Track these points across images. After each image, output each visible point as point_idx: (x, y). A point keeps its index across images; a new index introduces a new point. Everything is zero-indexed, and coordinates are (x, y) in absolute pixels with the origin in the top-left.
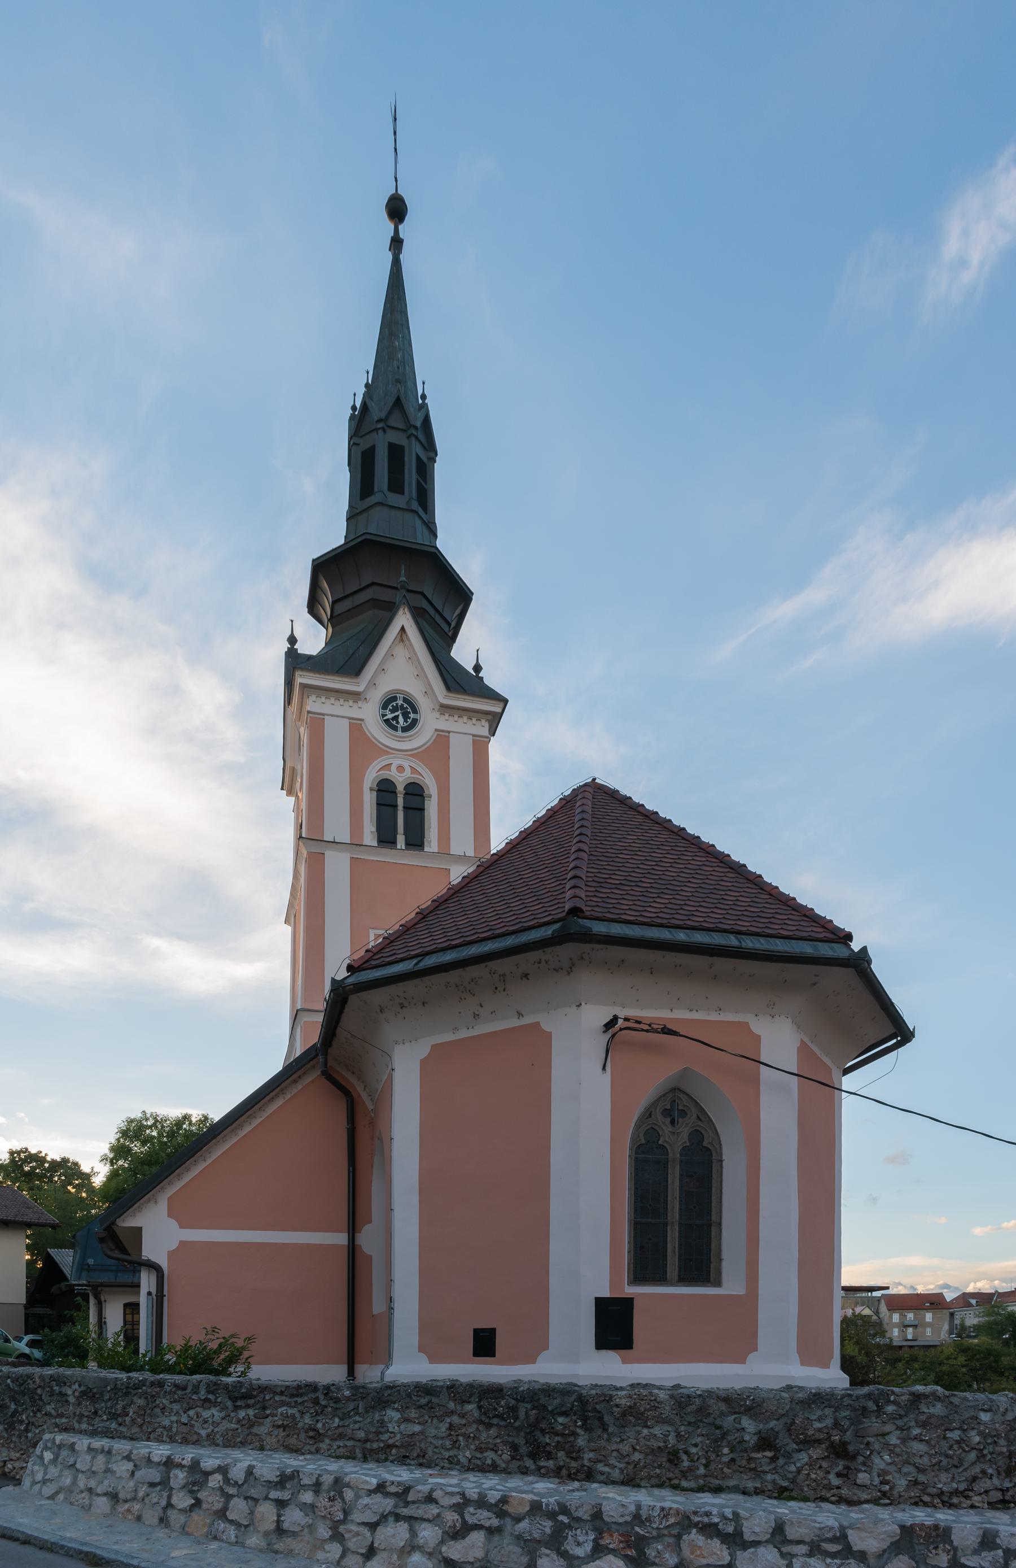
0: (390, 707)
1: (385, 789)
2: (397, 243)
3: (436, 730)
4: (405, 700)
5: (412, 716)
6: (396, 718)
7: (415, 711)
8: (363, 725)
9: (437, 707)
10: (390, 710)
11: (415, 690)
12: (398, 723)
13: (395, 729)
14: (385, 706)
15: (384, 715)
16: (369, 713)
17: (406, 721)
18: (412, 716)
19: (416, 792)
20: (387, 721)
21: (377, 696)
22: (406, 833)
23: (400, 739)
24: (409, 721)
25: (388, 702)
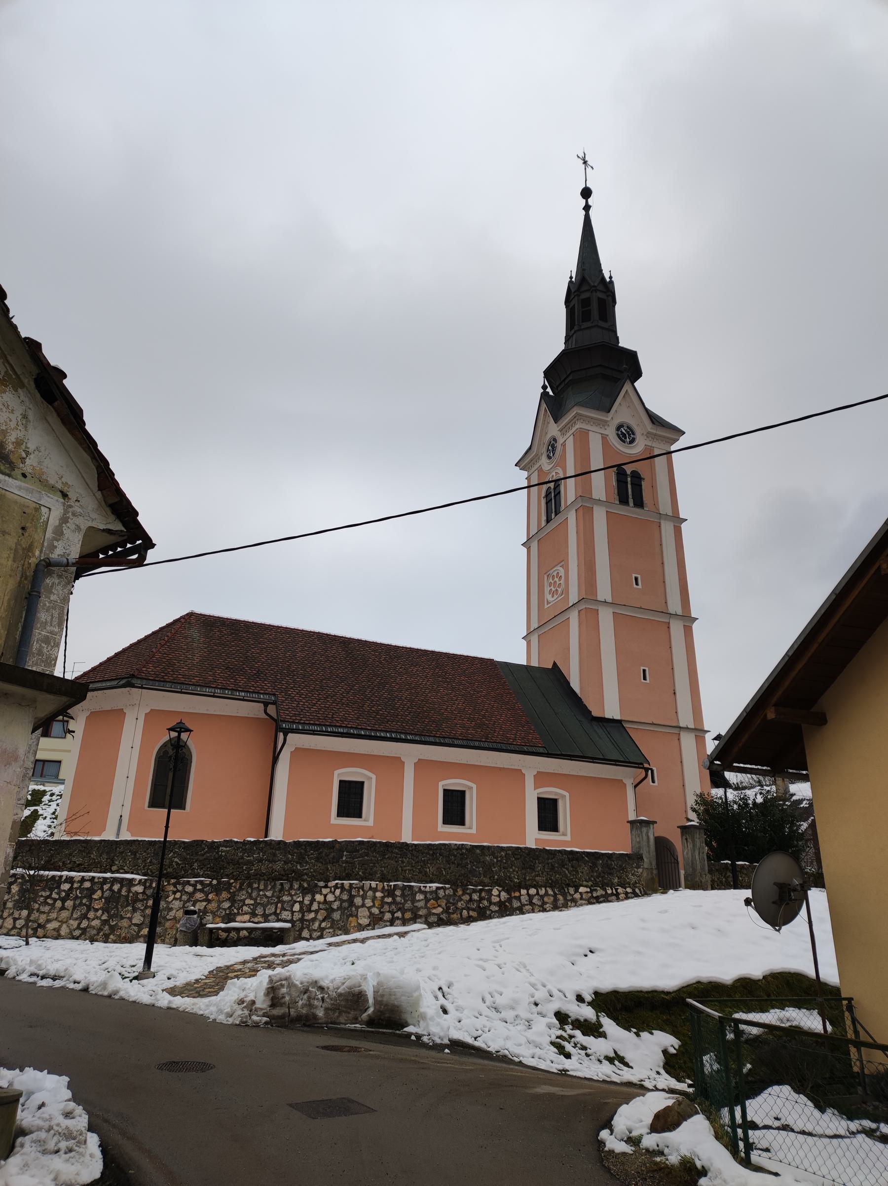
2: (587, 208)
4: (628, 427)
11: (633, 423)
16: (611, 433)
23: (631, 448)
24: (631, 438)
25: (619, 428)
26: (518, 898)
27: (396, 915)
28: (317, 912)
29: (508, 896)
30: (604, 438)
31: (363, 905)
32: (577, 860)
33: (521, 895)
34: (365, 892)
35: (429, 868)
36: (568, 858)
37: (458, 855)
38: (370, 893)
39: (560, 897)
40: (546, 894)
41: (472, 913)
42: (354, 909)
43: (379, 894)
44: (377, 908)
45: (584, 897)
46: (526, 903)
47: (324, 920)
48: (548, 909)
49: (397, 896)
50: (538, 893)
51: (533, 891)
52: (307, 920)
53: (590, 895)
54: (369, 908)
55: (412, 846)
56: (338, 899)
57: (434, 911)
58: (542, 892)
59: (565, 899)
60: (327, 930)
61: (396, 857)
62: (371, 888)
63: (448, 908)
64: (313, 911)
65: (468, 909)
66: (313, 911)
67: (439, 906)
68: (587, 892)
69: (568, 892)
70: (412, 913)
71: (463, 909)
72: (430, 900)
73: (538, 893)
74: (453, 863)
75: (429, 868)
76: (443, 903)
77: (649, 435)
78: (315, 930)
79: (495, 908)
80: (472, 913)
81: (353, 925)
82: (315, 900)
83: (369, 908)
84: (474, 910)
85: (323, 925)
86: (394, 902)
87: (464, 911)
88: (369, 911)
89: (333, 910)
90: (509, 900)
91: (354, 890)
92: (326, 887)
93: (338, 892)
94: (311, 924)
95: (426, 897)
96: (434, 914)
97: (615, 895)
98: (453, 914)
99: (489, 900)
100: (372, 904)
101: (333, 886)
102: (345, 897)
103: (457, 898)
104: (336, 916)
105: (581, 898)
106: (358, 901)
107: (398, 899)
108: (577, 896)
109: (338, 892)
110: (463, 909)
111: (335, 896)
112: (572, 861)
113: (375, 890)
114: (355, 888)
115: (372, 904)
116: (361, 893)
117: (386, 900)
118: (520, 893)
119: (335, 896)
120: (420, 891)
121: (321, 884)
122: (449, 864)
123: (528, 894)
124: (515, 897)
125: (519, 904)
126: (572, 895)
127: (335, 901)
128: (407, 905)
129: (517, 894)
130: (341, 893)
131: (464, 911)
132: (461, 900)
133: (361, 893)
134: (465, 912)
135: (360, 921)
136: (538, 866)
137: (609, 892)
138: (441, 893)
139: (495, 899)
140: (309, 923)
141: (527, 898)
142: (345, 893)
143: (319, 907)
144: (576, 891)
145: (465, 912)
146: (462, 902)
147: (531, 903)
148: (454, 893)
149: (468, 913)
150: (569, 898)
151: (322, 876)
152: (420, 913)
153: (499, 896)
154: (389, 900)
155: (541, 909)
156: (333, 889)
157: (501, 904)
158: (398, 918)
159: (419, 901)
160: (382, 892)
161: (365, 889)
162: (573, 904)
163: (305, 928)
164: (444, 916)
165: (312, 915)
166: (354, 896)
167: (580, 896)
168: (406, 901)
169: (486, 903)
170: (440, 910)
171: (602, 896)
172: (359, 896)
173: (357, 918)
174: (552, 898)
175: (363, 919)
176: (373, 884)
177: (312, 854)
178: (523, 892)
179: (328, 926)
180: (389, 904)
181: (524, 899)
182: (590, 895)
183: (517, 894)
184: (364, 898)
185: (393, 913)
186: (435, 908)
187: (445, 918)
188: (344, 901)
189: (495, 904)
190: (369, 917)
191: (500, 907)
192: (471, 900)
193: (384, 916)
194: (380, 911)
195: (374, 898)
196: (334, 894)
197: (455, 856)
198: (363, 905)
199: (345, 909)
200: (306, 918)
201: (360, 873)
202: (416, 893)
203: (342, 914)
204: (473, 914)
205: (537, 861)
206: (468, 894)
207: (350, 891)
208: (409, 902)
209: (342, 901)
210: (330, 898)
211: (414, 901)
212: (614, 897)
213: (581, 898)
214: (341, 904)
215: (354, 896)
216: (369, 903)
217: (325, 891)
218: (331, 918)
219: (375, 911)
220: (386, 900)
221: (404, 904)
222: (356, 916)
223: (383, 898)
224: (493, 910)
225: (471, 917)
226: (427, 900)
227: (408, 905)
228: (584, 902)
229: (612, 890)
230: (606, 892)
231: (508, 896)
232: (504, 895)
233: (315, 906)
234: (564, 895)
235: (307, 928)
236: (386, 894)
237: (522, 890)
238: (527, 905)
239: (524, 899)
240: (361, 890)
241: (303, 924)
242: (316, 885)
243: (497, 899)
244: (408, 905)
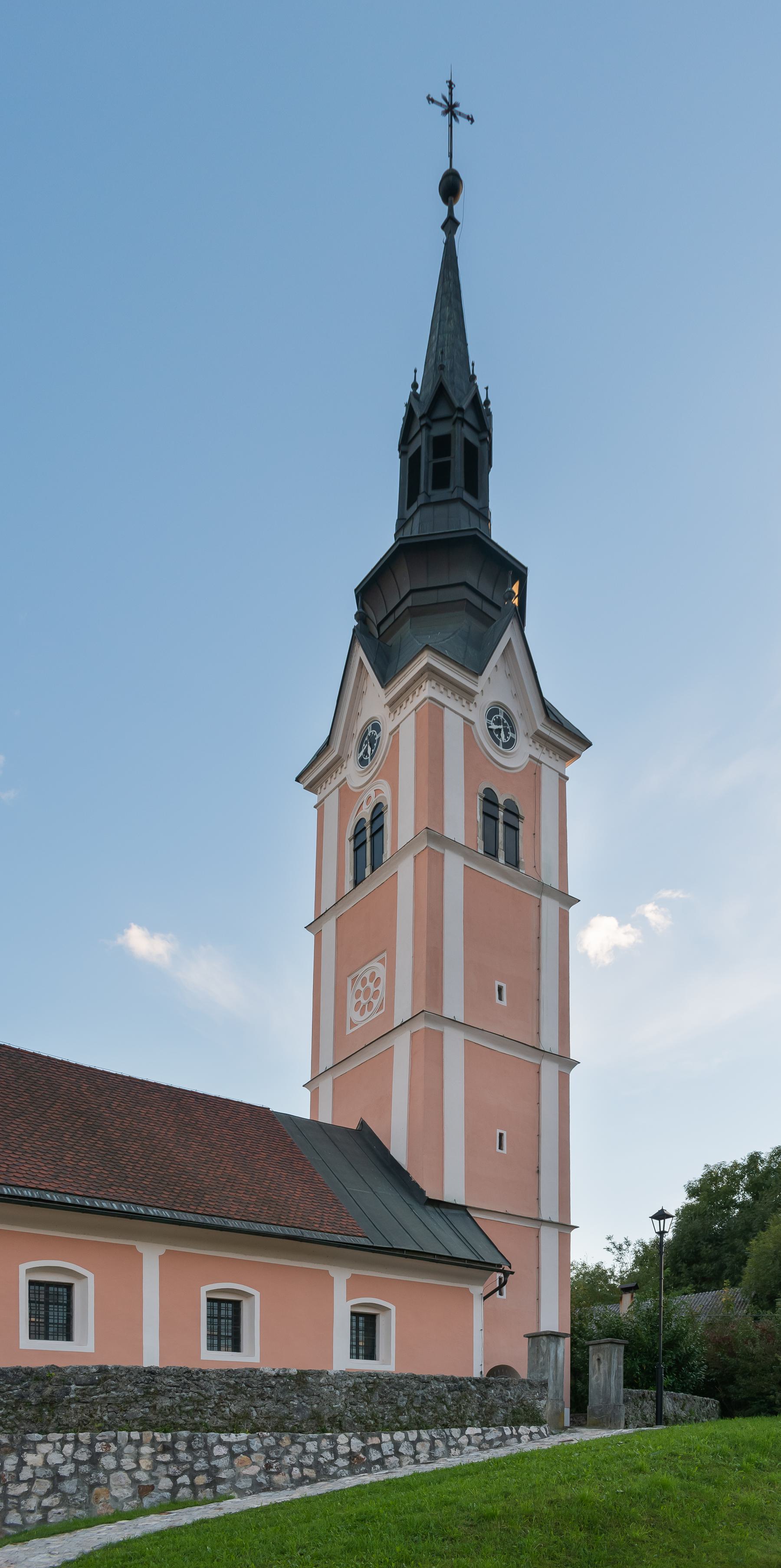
0: (493, 718)
1: (489, 799)
3: (530, 756)
4: (505, 716)
5: (510, 733)
6: (499, 731)
7: (513, 731)
8: (472, 728)
9: (531, 733)
10: (494, 722)
11: (514, 708)
12: (500, 737)
13: (498, 742)
14: (489, 716)
15: (488, 725)
16: (478, 716)
17: (506, 738)
18: (510, 733)
19: (512, 811)
20: (491, 730)
21: (485, 701)
22: (505, 850)
24: (509, 738)
26: (378, 1447)
27: (180, 1480)
28: (30, 1482)
29: (363, 1445)
30: (468, 723)
31: (119, 1468)
32: (460, 1388)
33: (381, 1442)
34: (120, 1449)
35: (228, 1406)
36: (448, 1387)
37: (278, 1386)
38: (129, 1449)
39: (440, 1444)
40: (419, 1439)
41: (306, 1472)
42: (101, 1475)
43: (146, 1450)
44: (145, 1471)
45: (473, 1441)
46: (389, 1453)
47: (48, 1494)
48: (422, 1461)
49: (178, 1451)
50: (406, 1439)
51: (399, 1436)
52: (14, 1497)
53: (481, 1438)
54: (129, 1472)
55: (197, 1373)
56: (69, 1461)
57: (245, 1472)
58: (413, 1435)
59: (449, 1448)
60: (54, 1510)
61: (170, 1391)
62: (130, 1441)
63: (268, 1466)
64: (24, 1481)
65: (301, 1466)
66: (24, 1481)
67: (254, 1464)
68: (478, 1434)
69: (451, 1436)
70: (208, 1476)
71: (293, 1466)
72: (238, 1455)
73: (406, 1439)
74: (270, 1398)
75: (228, 1406)
76: (259, 1458)
77: (539, 737)
78: (32, 1512)
79: (342, 1462)
80: (306, 1472)
81: (102, 1499)
82: (25, 1464)
83: (129, 1472)
84: (310, 1467)
85: (46, 1502)
86: (176, 1461)
87: (295, 1469)
88: (130, 1477)
89: (62, 1479)
90: (365, 1450)
91: (98, 1444)
92: (45, 1441)
93: (68, 1449)
94: (23, 1502)
95: (231, 1452)
96: (245, 1476)
97: (515, 1436)
98: (277, 1473)
99: (334, 1451)
100: (135, 1466)
101: (59, 1441)
102: (83, 1455)
103: (281, 1451)
104: (69, 1486)
105: (469, 1444)
106: (108, 1462)
107: (183, 1456)
108: (464, 1440)
109: (68, 1449)
110: (293, 1466)
111: (64, 1456)
112: (453, 1391)
113: (139, 1443)
114: (101, 1441)
115: (135, 1466)
116: (114, 1448)
117: (160, 1458)
118: (380, 1438)
119: (64, 1456)
120: (220, 1442)
121: (37, 1437)
122: (263, 1400)
123: (392, 1439)
124: (373, 1446)
125: (379, 1456)
126: (455, 1439)
127: (64, 1463)
128: (197, 1464)
129: (376, 1440)
130: (76, 1449)
131: (295, 1469)
132: (288, 1452)
133: (114, 1448)
134: (296, 1472)
135: (115, 1493)
136: (403, 1401)
137: (508, 1432)
138: (256, 1444)
139: (343, 1450)
140: (19, 1501)
141: (391, 1446)
142: (83, 1449)
143: (34, 1474)
144: (463, 1433)
145: (296, 1472)
146: (291, 1456)
147: (398, 1454)
148: (278, 1444)
149: (302, 1471)
150: (452, 1443)
151: (33, 1426)
152: (223, 1475)
153: (349, 1444)
154: (167, 1457)
155: (413, 1461)
156: (58, 1444)
157: (351, 1456)
158: (183, 1485)
159: (219, 1457)
160: (152, 1447)
161: (120, 1442)
162: (458, 1452)
163: (10, 1510)
164: (262, 1479)
165: (24, 1488)
166: (99, 1455)
167: (467, 1440)
168: (196, 1459)
169: (328, 1456)
170: (255, 1470)
171: (498, 1439)
172: (109, 1454)
173: (110, 1488)
174: (428, 1445)
175: (120, 1490)
176: (135, 1435)
177: (9, 1389)
178: (386, 1437)
179: (55, 1504)
180: (166, 1464)
181: (387, 1448)
182: (481, 1438)
183: (376, 1440)
184: (118, 1456)
185: (174, 1478)
186: (246, 1467)
187: (264, 1482)
188: (83, 1463)
189: (343, 1456)
190: (132, 1485)
191: (350, 1459)
192: (305, 1452)
193: (157, 1483)
194: (150, 1475)
195: (137, 1458)
196: (61, 1452)
197: (272, 1387)
198: (119, 1468)
199: (85, 1475)
200: (10, 1493)
201: (105, 1418)
202: (213, 1445)
203: (82, 1483)
204: (310, 1473)
205: (401, 1393)
206: (299, 1443)
207: (91, 1446)
208: (202, 1460)
209: (78, 1463)
210: (55, 1459)
211: (209, 1458)
212: (514, 1440)
213: (469, 1444)
214: (77, 1468)
215: (99, 1455)
216: (128, 1463)
217: (44, 1448)
218: (59, 1491)
219: (142, 1476)
220: (160, 1458)
221: (192, 1464)
222: (107, 1485)
223: (154, 1455)
224: (340, 1465)
225: (306, 1477)
226: (233, 1455)
227: (201, 1465)
228: (472, 1448)
229: (511, 1429)
230: (504, 1433)
231: (363, 1445)
232: (357, 1445)
233: (26, 1474)
234: (445, 1439)
235: (16, 1508)
236: (160, 1448)
237: (383, 1435)
238: (391, 1456)
239: (387, 1448)
240: (112, 1444)
241: (6, 1502)
242: (24, 1441)
243: (347, 1450)
244: (201, 1465)
